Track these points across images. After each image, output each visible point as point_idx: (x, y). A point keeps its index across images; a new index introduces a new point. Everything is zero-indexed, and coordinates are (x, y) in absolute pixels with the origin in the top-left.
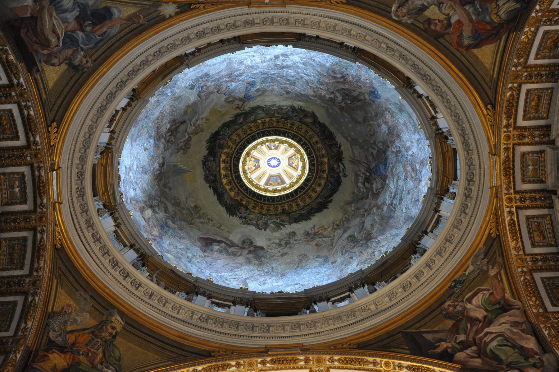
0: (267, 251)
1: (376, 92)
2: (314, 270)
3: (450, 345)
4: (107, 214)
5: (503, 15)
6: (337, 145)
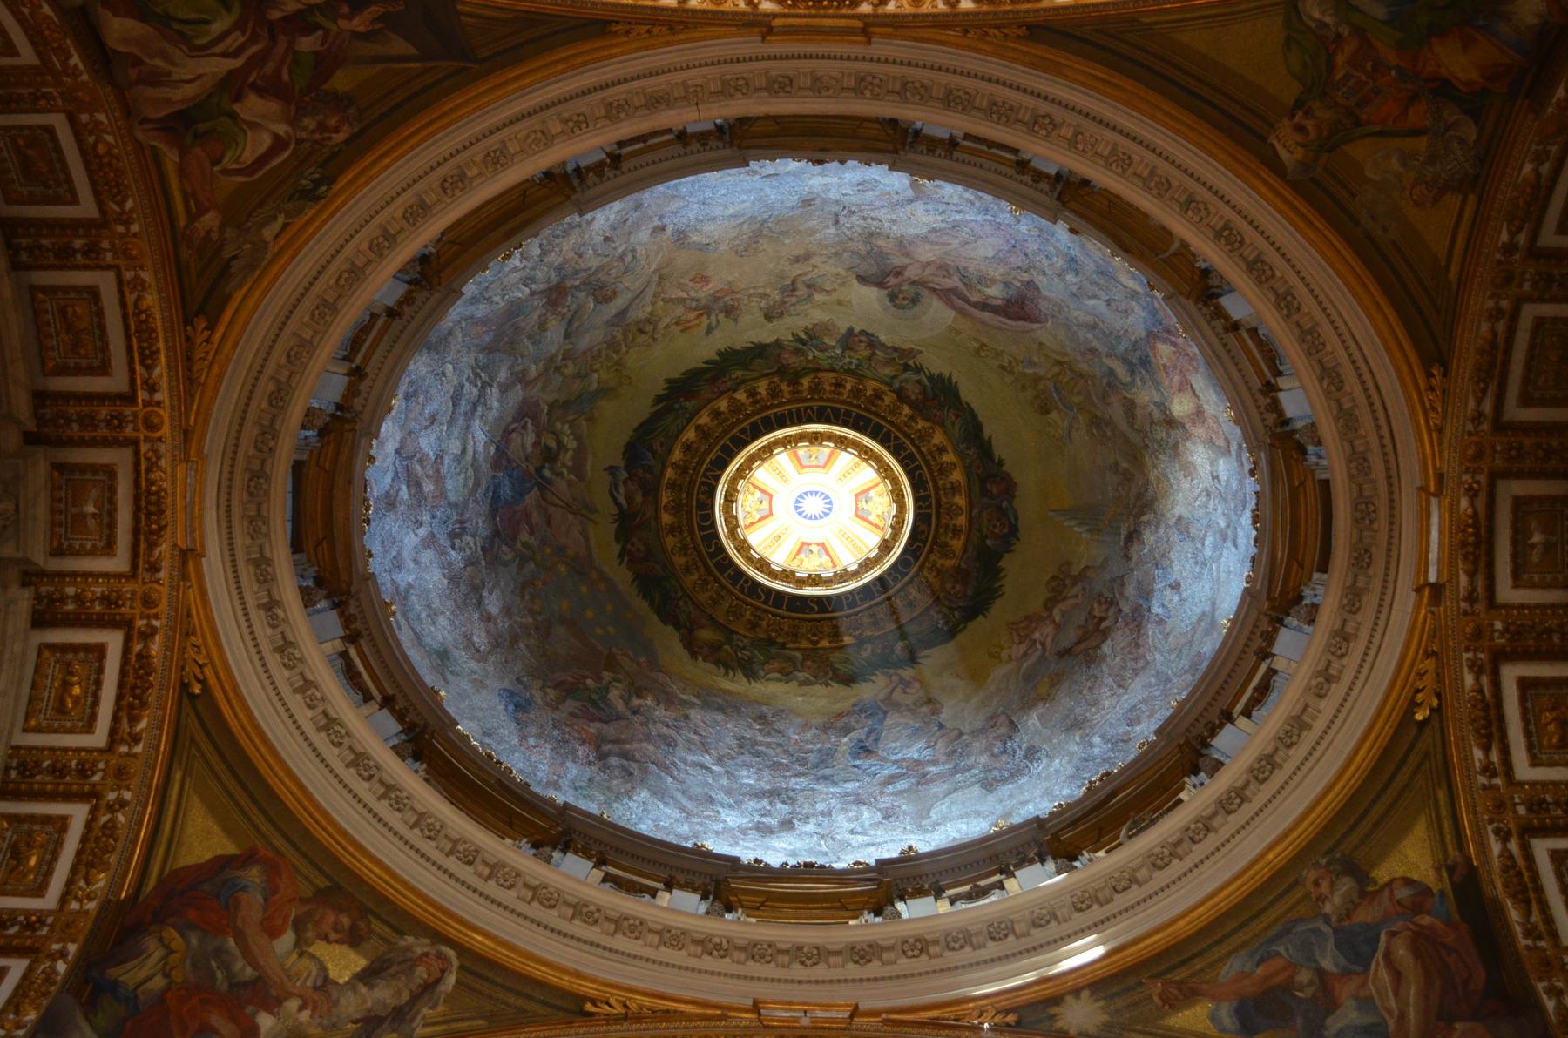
0: (848, 270)
1: (511, 707)
2: (718, 211)
3: (343, 23)
4: (1299, 425)
5: (152, 947)
6: (630, 561)
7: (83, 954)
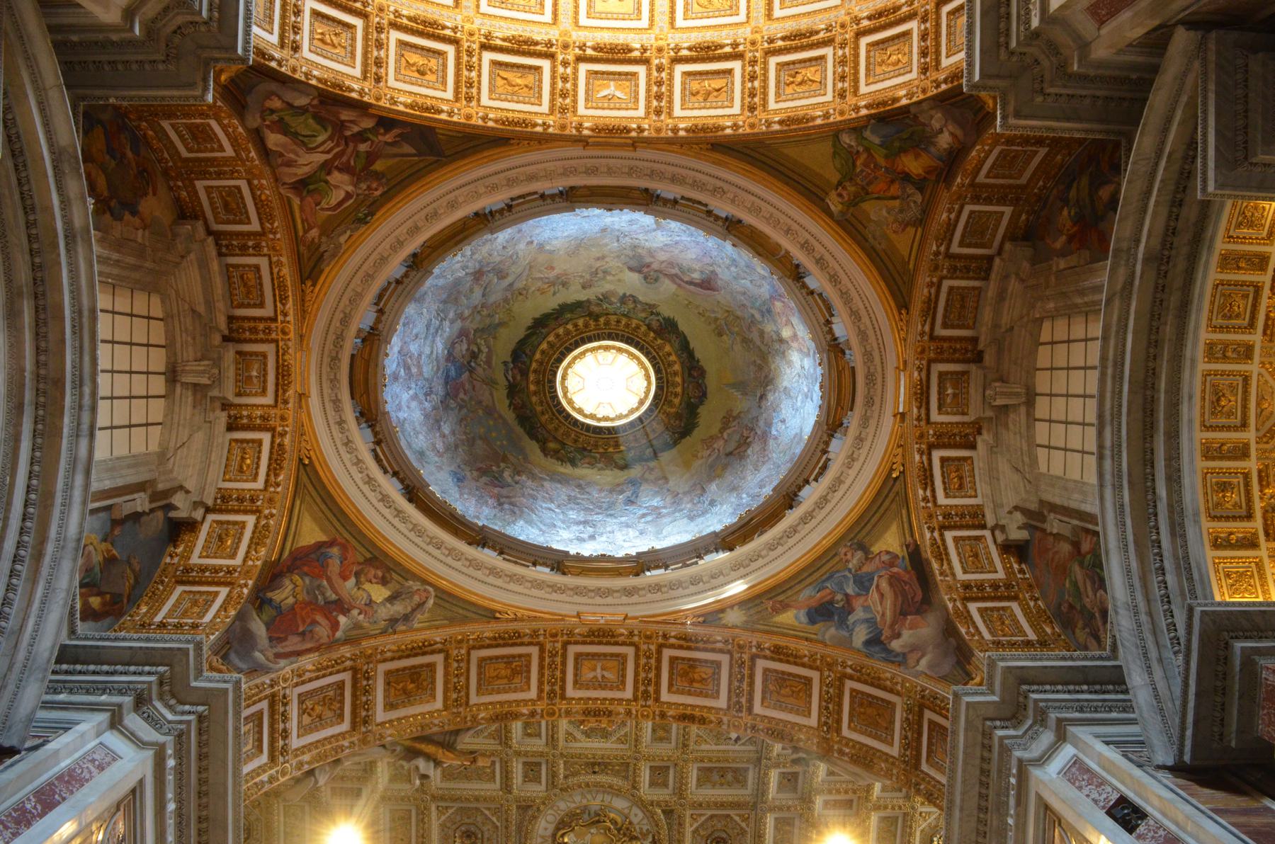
2: (559, 234)
3: (380, 138)
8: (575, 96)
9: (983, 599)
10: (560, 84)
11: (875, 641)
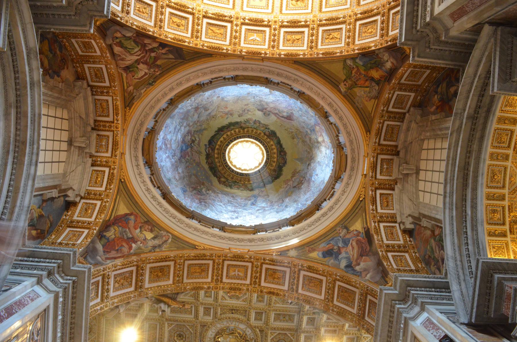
2: (230, 94)
3: (160, 51)
7: (99, 230)
8: (240, 38)
9: (394, 252)
10: (234, 34)
11: (349, 266)
